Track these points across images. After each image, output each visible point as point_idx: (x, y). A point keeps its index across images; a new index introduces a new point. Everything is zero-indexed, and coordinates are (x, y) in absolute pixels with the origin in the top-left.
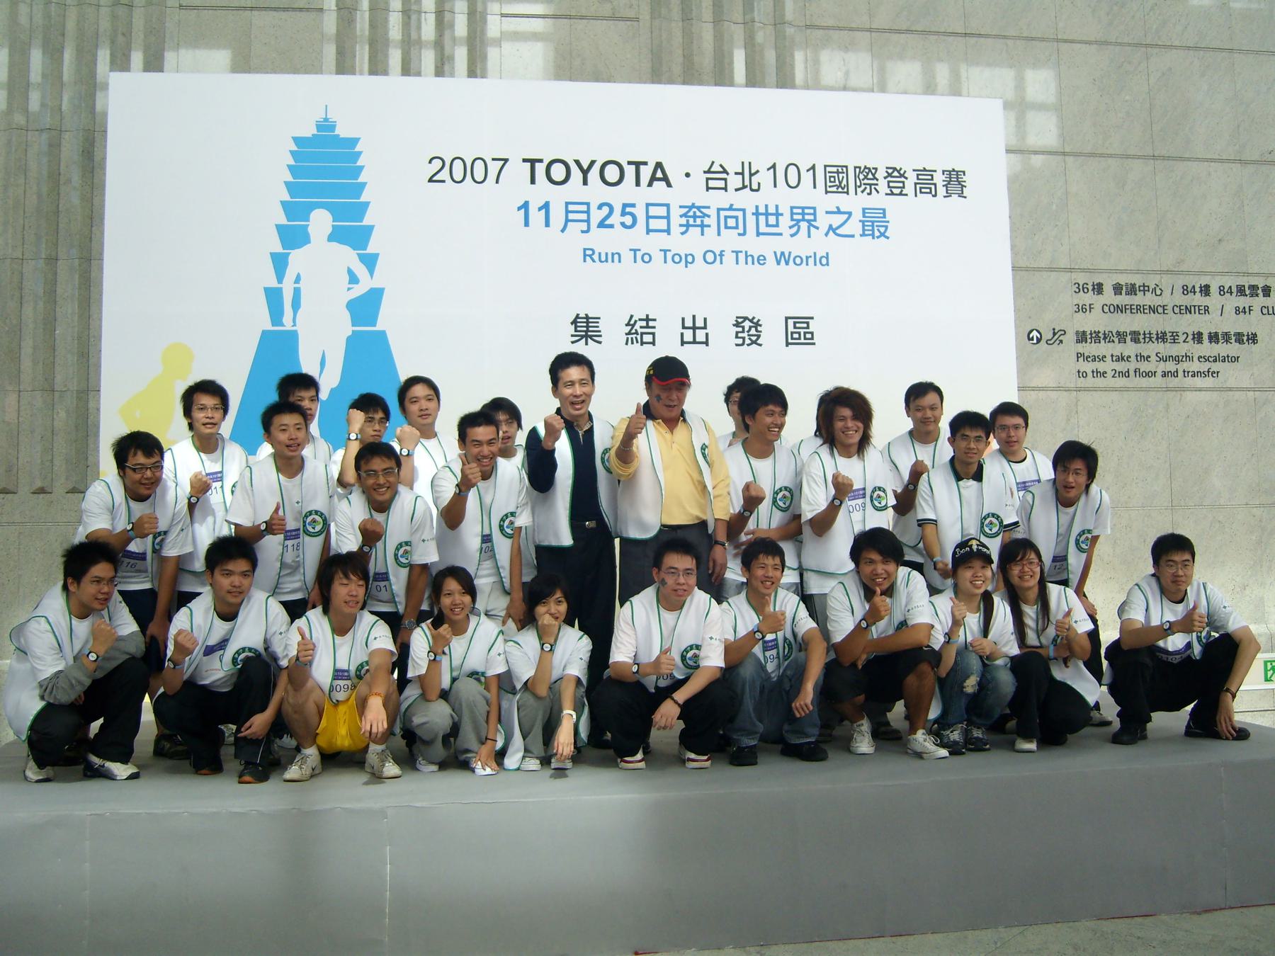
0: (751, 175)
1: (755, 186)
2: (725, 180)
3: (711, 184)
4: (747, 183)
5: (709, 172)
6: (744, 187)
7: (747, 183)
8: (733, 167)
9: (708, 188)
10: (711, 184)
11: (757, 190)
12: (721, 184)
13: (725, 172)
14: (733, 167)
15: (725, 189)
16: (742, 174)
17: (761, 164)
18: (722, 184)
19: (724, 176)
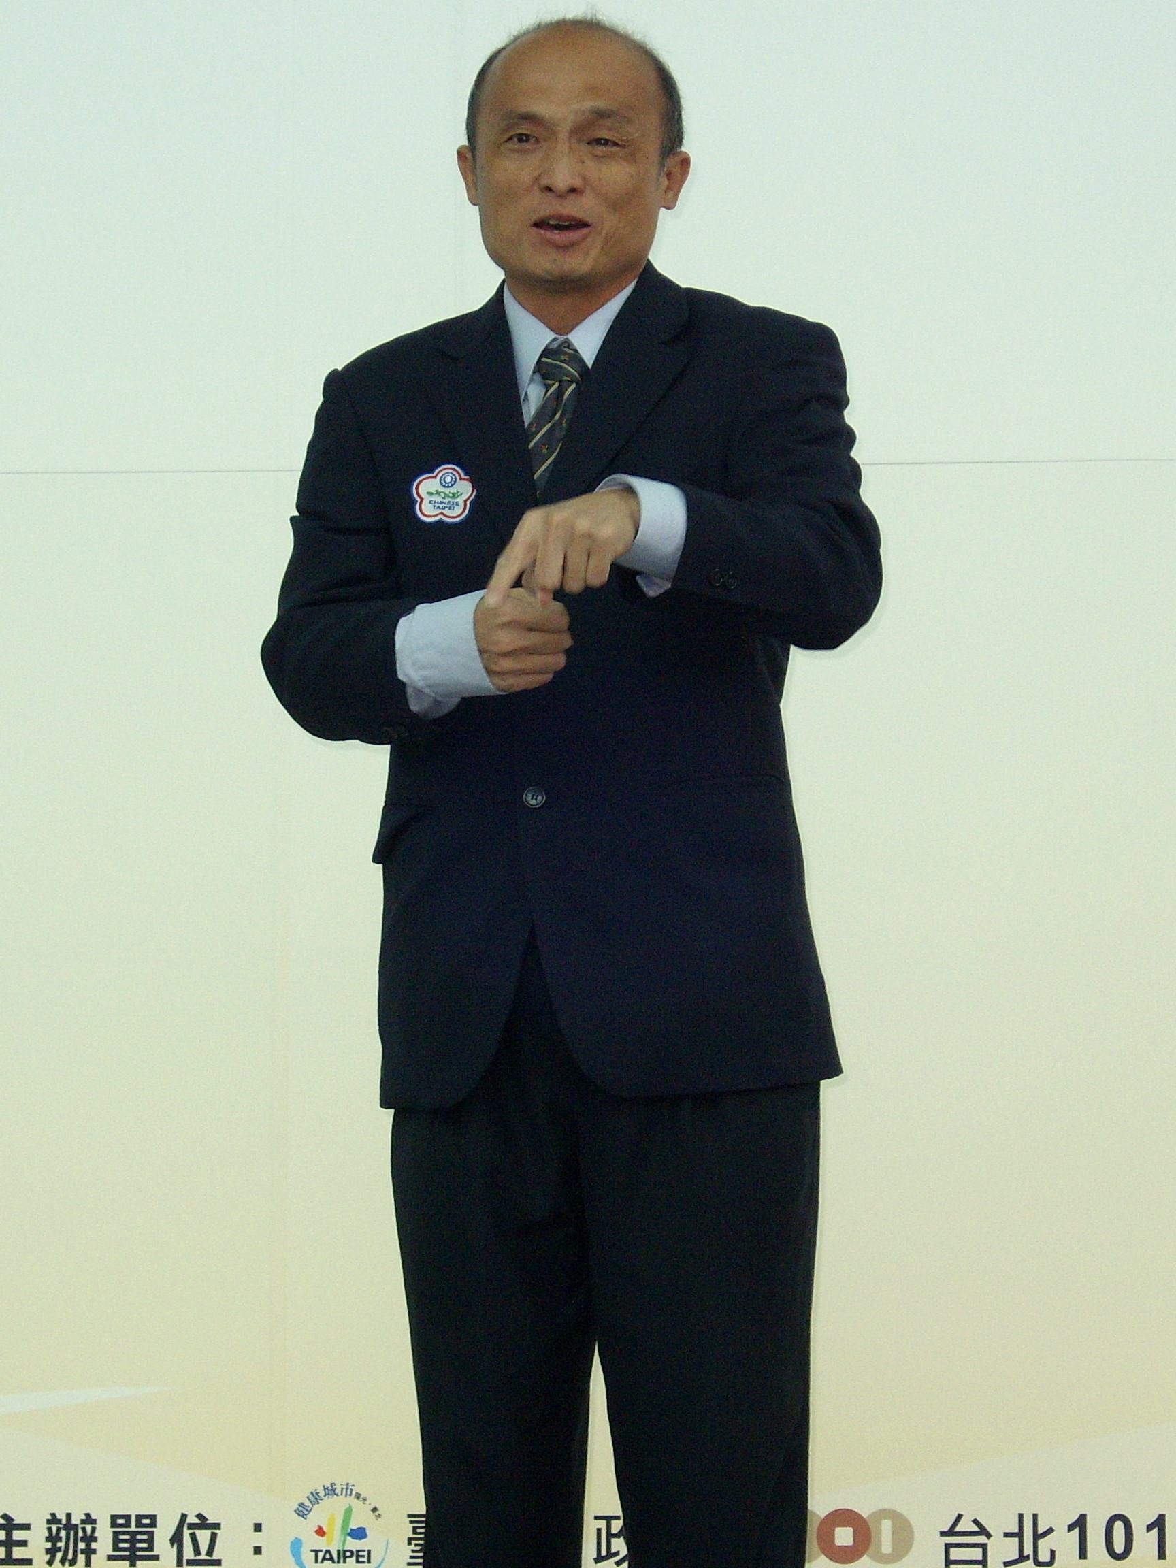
0: (1037, 1537)
1: (1044, 1556)
2: (984, 1547)
3: (955, 1554)
4: (1028, 1550)
5: (951, 1532)
6: (1022, 1558)
7: (1028, 1550)
8: (1000, 1522)
9: (948, 1562)
10: (955, 1554)
11: (1051, 1563)
12: (977, 1554)
13: (983, 1531)
14: (1000, 1522)
15: (984, 1562)
16: (1019, 1535)
17: (1057, 1517)
18: (977, 1554)
19: (981, 1539)
